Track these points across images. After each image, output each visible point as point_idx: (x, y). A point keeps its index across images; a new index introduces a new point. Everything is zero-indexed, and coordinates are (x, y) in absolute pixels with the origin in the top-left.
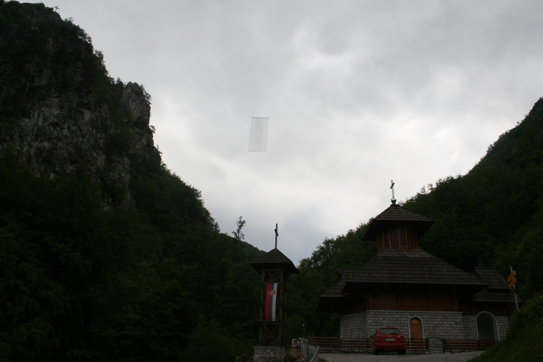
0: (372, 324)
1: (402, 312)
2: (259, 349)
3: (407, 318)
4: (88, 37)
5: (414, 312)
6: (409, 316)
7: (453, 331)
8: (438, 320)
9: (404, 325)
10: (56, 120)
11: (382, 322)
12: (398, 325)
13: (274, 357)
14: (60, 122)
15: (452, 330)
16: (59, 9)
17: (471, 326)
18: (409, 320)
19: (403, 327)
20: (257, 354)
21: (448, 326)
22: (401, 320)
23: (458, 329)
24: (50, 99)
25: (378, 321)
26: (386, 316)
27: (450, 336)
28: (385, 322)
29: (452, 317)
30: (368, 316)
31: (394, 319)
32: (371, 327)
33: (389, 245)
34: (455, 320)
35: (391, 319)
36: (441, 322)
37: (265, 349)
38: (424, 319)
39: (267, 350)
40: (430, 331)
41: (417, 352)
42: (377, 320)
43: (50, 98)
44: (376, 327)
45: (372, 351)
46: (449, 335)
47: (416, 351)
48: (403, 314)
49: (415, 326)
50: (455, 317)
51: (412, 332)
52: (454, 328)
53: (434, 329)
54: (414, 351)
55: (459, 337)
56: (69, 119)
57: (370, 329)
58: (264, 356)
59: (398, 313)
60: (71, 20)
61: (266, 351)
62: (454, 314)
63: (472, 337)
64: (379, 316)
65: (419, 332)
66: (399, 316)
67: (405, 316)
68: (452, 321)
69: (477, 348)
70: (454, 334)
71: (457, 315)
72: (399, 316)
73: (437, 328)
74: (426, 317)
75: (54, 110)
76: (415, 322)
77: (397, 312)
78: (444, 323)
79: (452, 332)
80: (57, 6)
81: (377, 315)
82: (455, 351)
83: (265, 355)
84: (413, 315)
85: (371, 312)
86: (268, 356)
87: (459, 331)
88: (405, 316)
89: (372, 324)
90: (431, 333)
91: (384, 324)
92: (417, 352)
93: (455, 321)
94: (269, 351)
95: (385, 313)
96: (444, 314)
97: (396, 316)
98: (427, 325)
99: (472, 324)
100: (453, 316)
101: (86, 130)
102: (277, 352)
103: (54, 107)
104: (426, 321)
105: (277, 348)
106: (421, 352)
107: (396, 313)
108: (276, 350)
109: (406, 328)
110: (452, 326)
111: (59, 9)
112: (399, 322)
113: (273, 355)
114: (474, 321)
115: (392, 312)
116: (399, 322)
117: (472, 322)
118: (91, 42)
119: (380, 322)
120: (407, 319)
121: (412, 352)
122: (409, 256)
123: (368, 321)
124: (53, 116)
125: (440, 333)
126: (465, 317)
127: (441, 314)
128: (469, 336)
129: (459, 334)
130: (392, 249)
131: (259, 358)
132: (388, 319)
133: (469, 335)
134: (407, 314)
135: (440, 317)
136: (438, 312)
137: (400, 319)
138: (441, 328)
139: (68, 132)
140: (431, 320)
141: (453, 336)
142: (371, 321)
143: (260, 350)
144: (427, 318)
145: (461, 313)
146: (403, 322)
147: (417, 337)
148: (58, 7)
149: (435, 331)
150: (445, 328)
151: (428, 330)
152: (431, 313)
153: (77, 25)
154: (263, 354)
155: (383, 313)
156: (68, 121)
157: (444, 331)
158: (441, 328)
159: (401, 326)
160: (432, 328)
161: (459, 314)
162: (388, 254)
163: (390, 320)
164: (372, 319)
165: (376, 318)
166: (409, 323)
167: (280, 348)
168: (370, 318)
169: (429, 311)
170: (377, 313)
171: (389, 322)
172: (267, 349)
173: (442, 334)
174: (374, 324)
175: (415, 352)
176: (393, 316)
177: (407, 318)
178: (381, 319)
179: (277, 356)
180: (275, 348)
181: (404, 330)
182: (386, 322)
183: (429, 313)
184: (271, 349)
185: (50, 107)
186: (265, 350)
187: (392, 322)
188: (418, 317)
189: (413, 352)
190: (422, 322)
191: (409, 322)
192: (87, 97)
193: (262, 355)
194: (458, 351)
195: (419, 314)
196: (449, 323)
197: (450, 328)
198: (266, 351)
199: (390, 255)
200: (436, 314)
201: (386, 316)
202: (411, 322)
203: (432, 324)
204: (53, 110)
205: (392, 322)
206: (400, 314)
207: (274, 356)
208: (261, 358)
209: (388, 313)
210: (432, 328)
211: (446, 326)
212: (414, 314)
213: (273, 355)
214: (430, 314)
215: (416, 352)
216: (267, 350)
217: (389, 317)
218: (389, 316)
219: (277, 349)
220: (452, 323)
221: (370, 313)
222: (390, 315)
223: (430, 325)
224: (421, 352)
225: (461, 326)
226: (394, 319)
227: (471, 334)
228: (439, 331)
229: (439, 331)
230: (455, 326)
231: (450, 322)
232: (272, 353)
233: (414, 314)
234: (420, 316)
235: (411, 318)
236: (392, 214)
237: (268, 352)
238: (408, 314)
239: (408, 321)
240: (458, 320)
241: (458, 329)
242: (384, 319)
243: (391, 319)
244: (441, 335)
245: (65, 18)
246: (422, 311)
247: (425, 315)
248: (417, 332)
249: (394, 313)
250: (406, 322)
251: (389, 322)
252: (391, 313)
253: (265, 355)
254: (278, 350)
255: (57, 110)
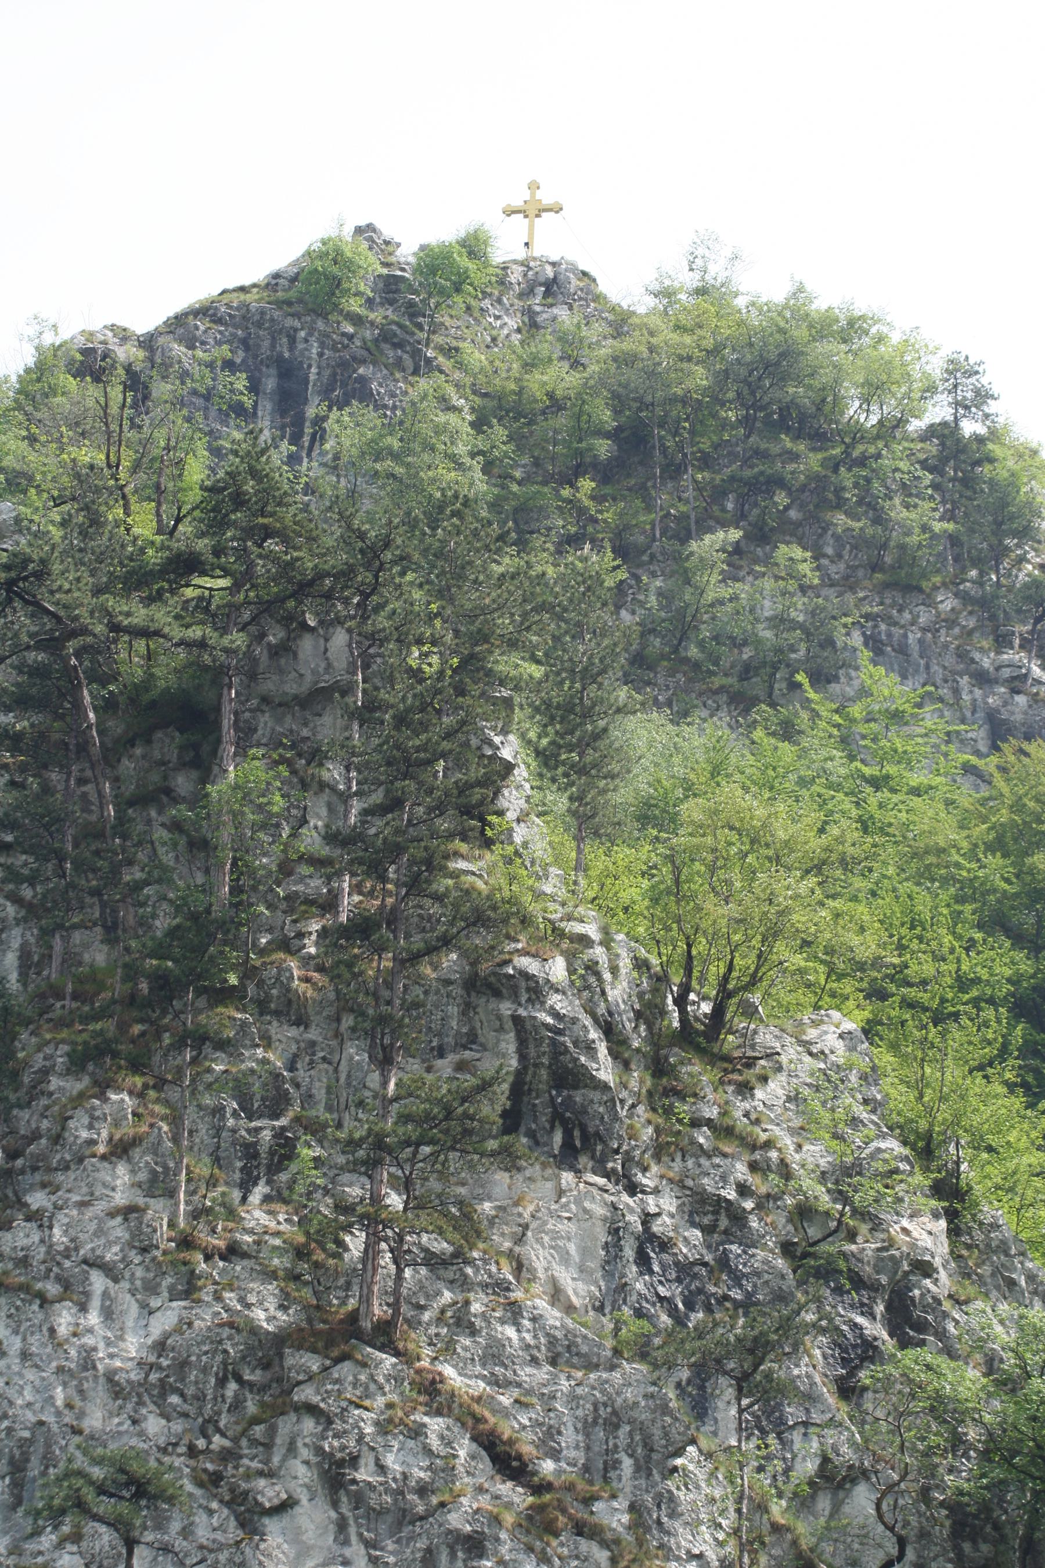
4: (935, 366)
10: (154, 1425)
14: (218, 1441)
16: (557, 209)
24: (37, 1200)
43: (44, 1185)
56: (314, 1363)
60: (717, 271)
75: (108, 1314)
80: (533, 186)
101: (587, 1427)
103: (98, 1282)
111: (557, 209)
118: (992, 407)
124: (116, 1389)
139: (342, 1526)
148: (546, 197)
153: (776, 293)
156: (307, 1394)
185: (52, 1289)
192: (506, 1008)
204: (93, 1318)
245: (650, 278)
255: (155, 1303)
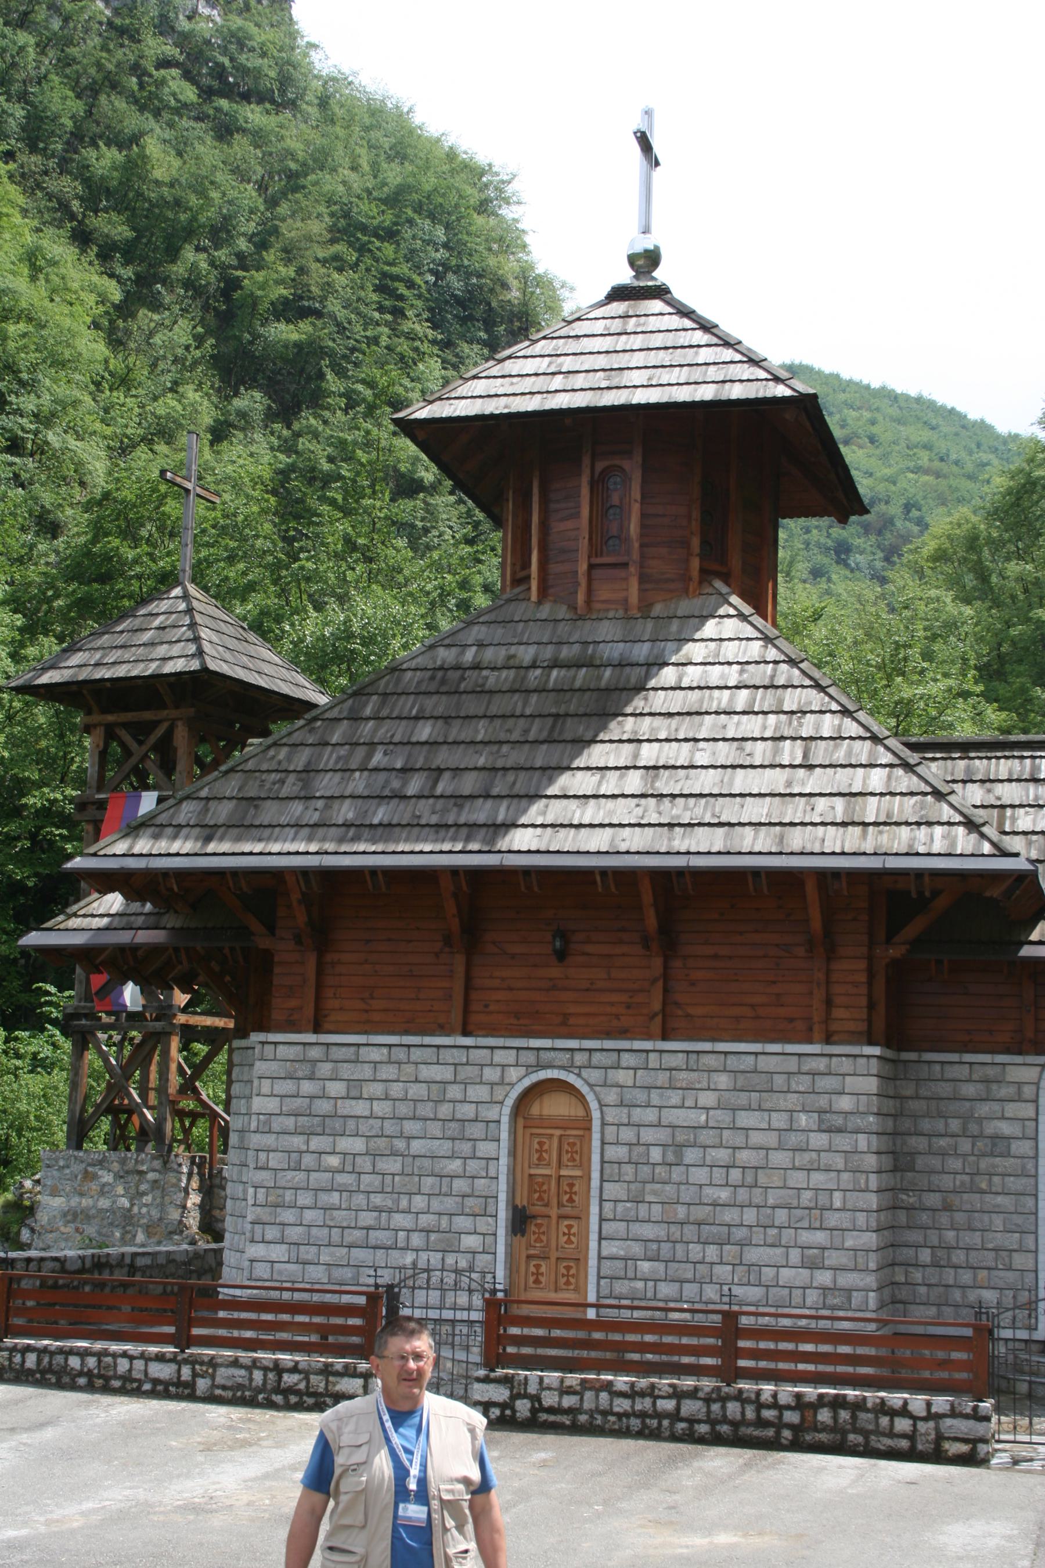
0: (277, 1124)
1: (468, 1047)
2: (61, 1163)
3: (502, 1083)
5: (547, 1043)
6: (513, 1074)
7: (797, 1179)
8: (707, 1099)
9: (476, 1130)
11: (340, 1112)
12: (435, 1129)
13: (130, 1210)
15: (794, 1168)
17: (1006, 1128)
18: (510, 1102)
19: (470, 1144)
20: (54, 1193)
21: (771, 1139)
22: (459, 1096)
23: (839, 1161)
25: (318, 1102)
26: (367, 1072)
27: (774, 1208)
28: (360, 1108)
29: (803, 1083)
30: (260, 1067)
31: (417, 1091)
32: (270, 1140)
33: (527, 578)
34: (823, 1102)
35: (396, 1090)
36: (722, 1117)
37: (89, 1165)
38: (611, 1096)
39: (100, 1173)
40: (646, 1169)
41: (286, 1377)
42: (312, 1097)
44: (298, 1141)
45: (10, 1359)
46: (771, 1201)
47: (278, 1369)
48: (477, 1055)
49: (558, 1132)
50: (825, 1083)
51: (533, 1171)
52: (807, 1156)
53: (671, 1158)
54: (265, 1369)
55: (833, 1219)
57: (262, 1156)
58: (85, 1202)
59: (447, 1055)
61: (95, 1177)
62: (821, 1064)
63: (1000, 1199)
64: (325, 1069)
65: (577, 1173)
66: (445, 1073)
67: (491, 1074)
68: (803, 1111)
69: (742, 1363)
70: (807, 1195)
71: (846, 1065)
72: (447, 1073)
73: (691, 1155)
74: (622, 1076)
76: (555, 1107)
77: (438, 1047)
78: (745, 1119)
79: (791, 1183)
81: (314, 1062)
82: (541, 1378)
83: (90, 1202)
84: (540, 1066)
85: (275, 1043)
86: (104, 1203)
87: (845, 1176)
88: (491, 1074)
89: (277, 1124)
90: (648, 1186)
91: (351, 1124)
92: (286, 1377)
93: (821, 1112)
94: (107, 1178)
95: (363, 1050)
96: (751, 1059)
97: (425, 1072)
98: (627, 1134)
99: (1011, 1109)
100: (814, 1074)
102: (143, 1187)
104: (621, 1104)
105: (143, 1163)
106: (313, 1378)
107: (429, 1054)
108: (141, 1173)
109: (485, 1148)
110: (794, 1139)
112: (444, 1110)
113: (127, 1205)
114: (1028, 1091)
115: (409, 1046)
116: (444, 1110)
117: (1019, 1099)
119: (323, 1106)
120: (499, 1093)
121: (251, 1380)
122: (613, 651)
123: (258, 1104)
125: (708, 1191)
126: (971, 1064)
127: (732, 1062)
128: (983, 1192)
129: (837, 1196)
130: (539, 603)
131: (65, 1215)
132: (377, 1089)
133: (984, 1186)
134: (500, 1057)
135: (723, 1080)
136: (707, 1046)
137: (454, 1092)
138: (722, 1155)
140: (655, 1098)
141: (798, 1213)
142: (272, 1105)
143: (67, 1171)
144: (634, 1086)
145: (876, 1051)
146: (467, 1111)
147: (560, 1205)
149: (677, 1173)
150: (744, 1156)
151: (629, 1169)
152: (661, 1052)
154: (82, 1195)
155: (349, 1053)
157: (735, 1175)
158: (722, 1155)
159: (453, 1139)
160: (656, 1154)
161: (862, 1061)
162: (481, 645)
163: (387, 1098)
164: (288, 1087)
165: (307, 1087)
166: (505, 1120)
167: (157, 1164)
168: (266, 1086)
169: (648, 1036)
170: (315, 1053)
171: (380, 1107)
172: (101, 1163)
173: (724, 1195)
174: (290, 1122)
175: (271, 1376)
176: (409, 1069)
177: (502, 1083)
178: (336, 1088)
179: (146, 1205)
180: (137, 1161)
181: (473, 1166)
182: (367, 1113)
183: (647, 1051)
184: (116, 1166)
186: (90, 1169)
187: (403, 1109)
188: (571, 1079)
189: (258, 1376)
190: (596, 1115)
191: (507, 1110)
193: (75, 1201)
194: (562, 1381)
195: (580, 1059)
196: (779, 1120)
197: (779, 1158)
198: (95, 1177)
199: (489, 655)
200: (694, 1056)
201: (367, 1072)
202: (535, 1110)
203: (659, 1125)
205: (403, 1109)
206: (461, 1056)
207: (132, 1205)
208: (72, 1216)
209: (385, 1050)
210: (656, 1154)
211: (756, 1138)
212: (545, 1056)
213: (125, 1202)
214: (652, 1055)
215: (280, 1377)
216: (100, 1173)
217: (384, 1077)
218: (388, 1072)
219: (144, 1168)
220: (803, 1120)
221: (269, 1048)
222: (389, 1062)
223: (648, 1135)
224: (313, 1378)
225: (862, 1141)
226: (417, 1091)
227: (996, 1179)
228: (700, 1175)
229: (700, 1175)
230: (819, 1140)
231: (785, 1116)
232: (120, 1190)
233: (545, 1056)
234: (585, 1073)
235: (527, 1082)
236: (568, 363)
237: (104, 1185)
238: (510, 1057)
239: (502, 1103)
240: (845, 1103)
241: (839, 1161)
242: (352, 1094)
243: (396, 1090)
244: (715, 1204)
246: (608, 1035)
247: (617, 1067)
248: (563, 1172)
249: (416, 1054)
250: (492, 1113)
251: (380, 1107)
252: (400, 1054)
253: (90, 1202)
254: (151, 1176)
